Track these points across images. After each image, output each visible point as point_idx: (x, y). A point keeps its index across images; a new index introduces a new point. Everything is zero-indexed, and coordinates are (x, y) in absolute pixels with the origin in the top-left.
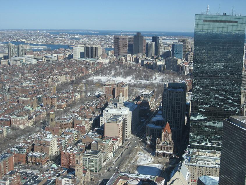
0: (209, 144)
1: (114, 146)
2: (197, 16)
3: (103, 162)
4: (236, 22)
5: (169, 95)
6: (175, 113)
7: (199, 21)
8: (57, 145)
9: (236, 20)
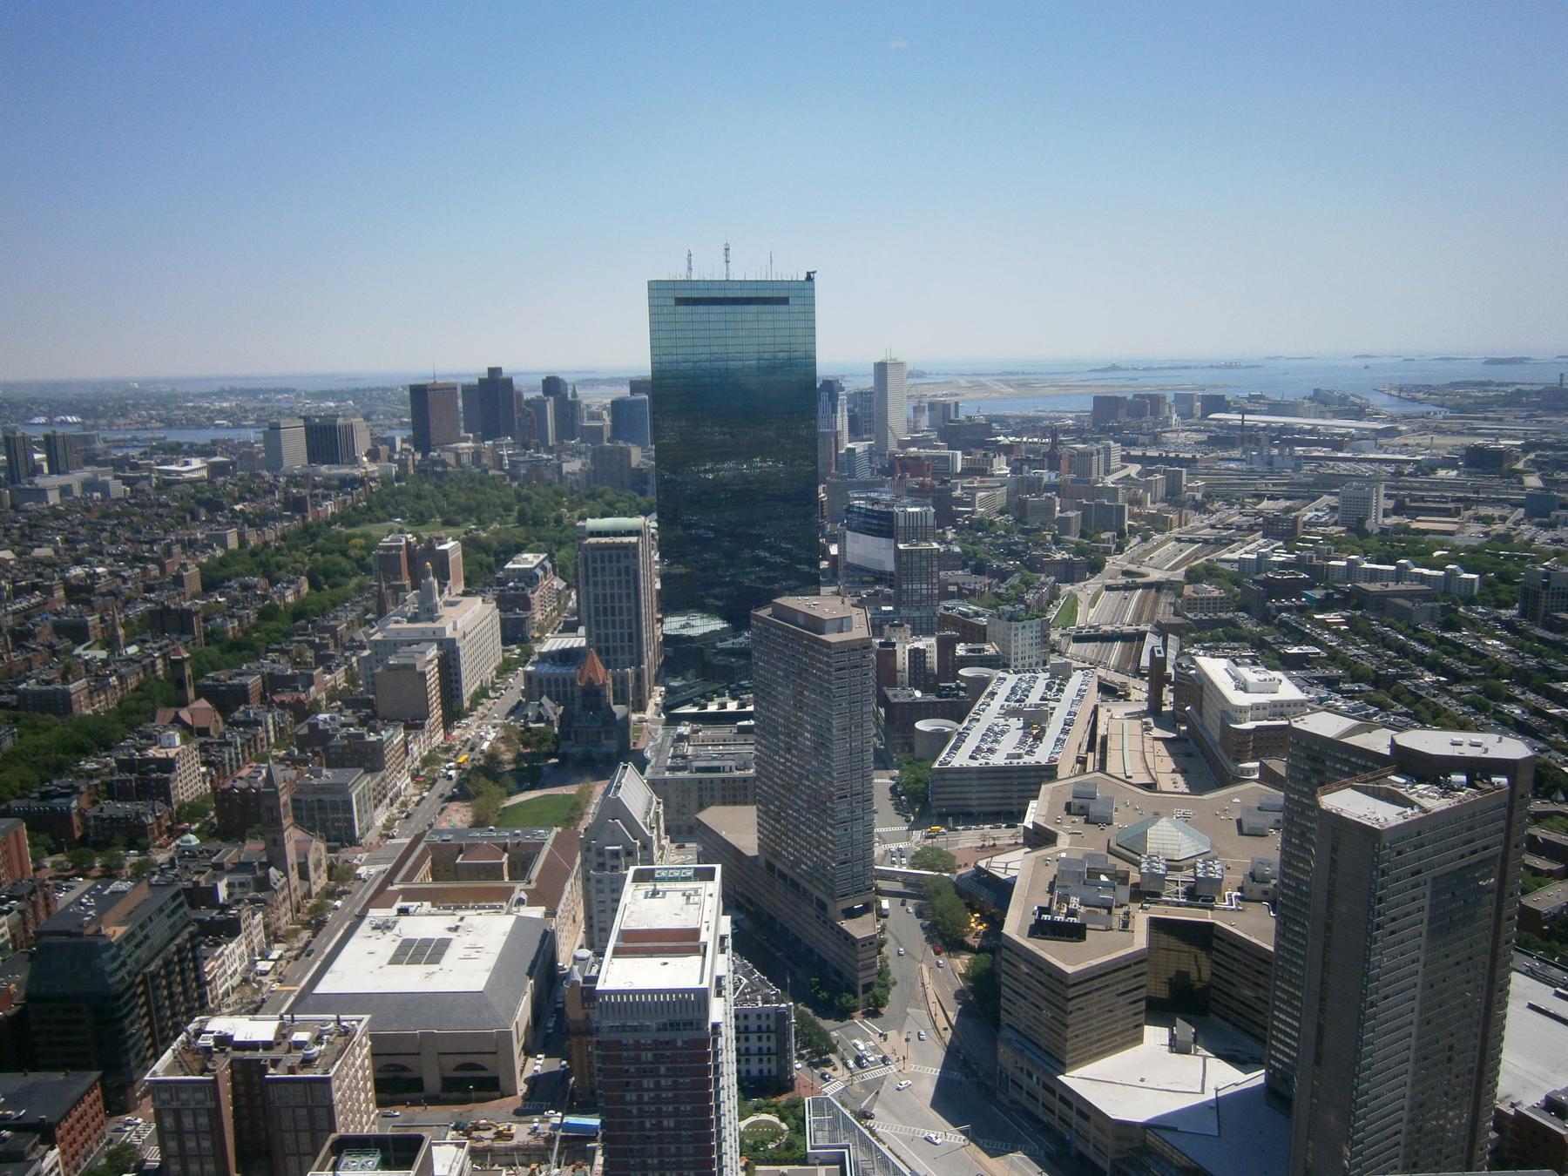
0: (732, 706)
1: (414, 747)
2: (656, 288)
3: (376, 807)
4: (784, 301)
5: (590, 561)
6: (610, 618)
7: (661, 302)
8: (203, 769)
9: (783, 294)
